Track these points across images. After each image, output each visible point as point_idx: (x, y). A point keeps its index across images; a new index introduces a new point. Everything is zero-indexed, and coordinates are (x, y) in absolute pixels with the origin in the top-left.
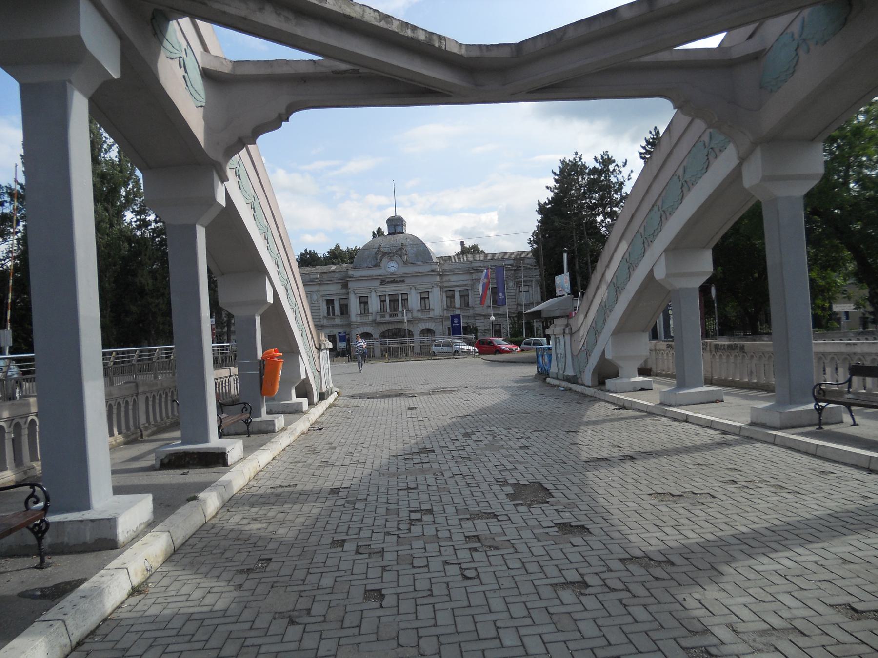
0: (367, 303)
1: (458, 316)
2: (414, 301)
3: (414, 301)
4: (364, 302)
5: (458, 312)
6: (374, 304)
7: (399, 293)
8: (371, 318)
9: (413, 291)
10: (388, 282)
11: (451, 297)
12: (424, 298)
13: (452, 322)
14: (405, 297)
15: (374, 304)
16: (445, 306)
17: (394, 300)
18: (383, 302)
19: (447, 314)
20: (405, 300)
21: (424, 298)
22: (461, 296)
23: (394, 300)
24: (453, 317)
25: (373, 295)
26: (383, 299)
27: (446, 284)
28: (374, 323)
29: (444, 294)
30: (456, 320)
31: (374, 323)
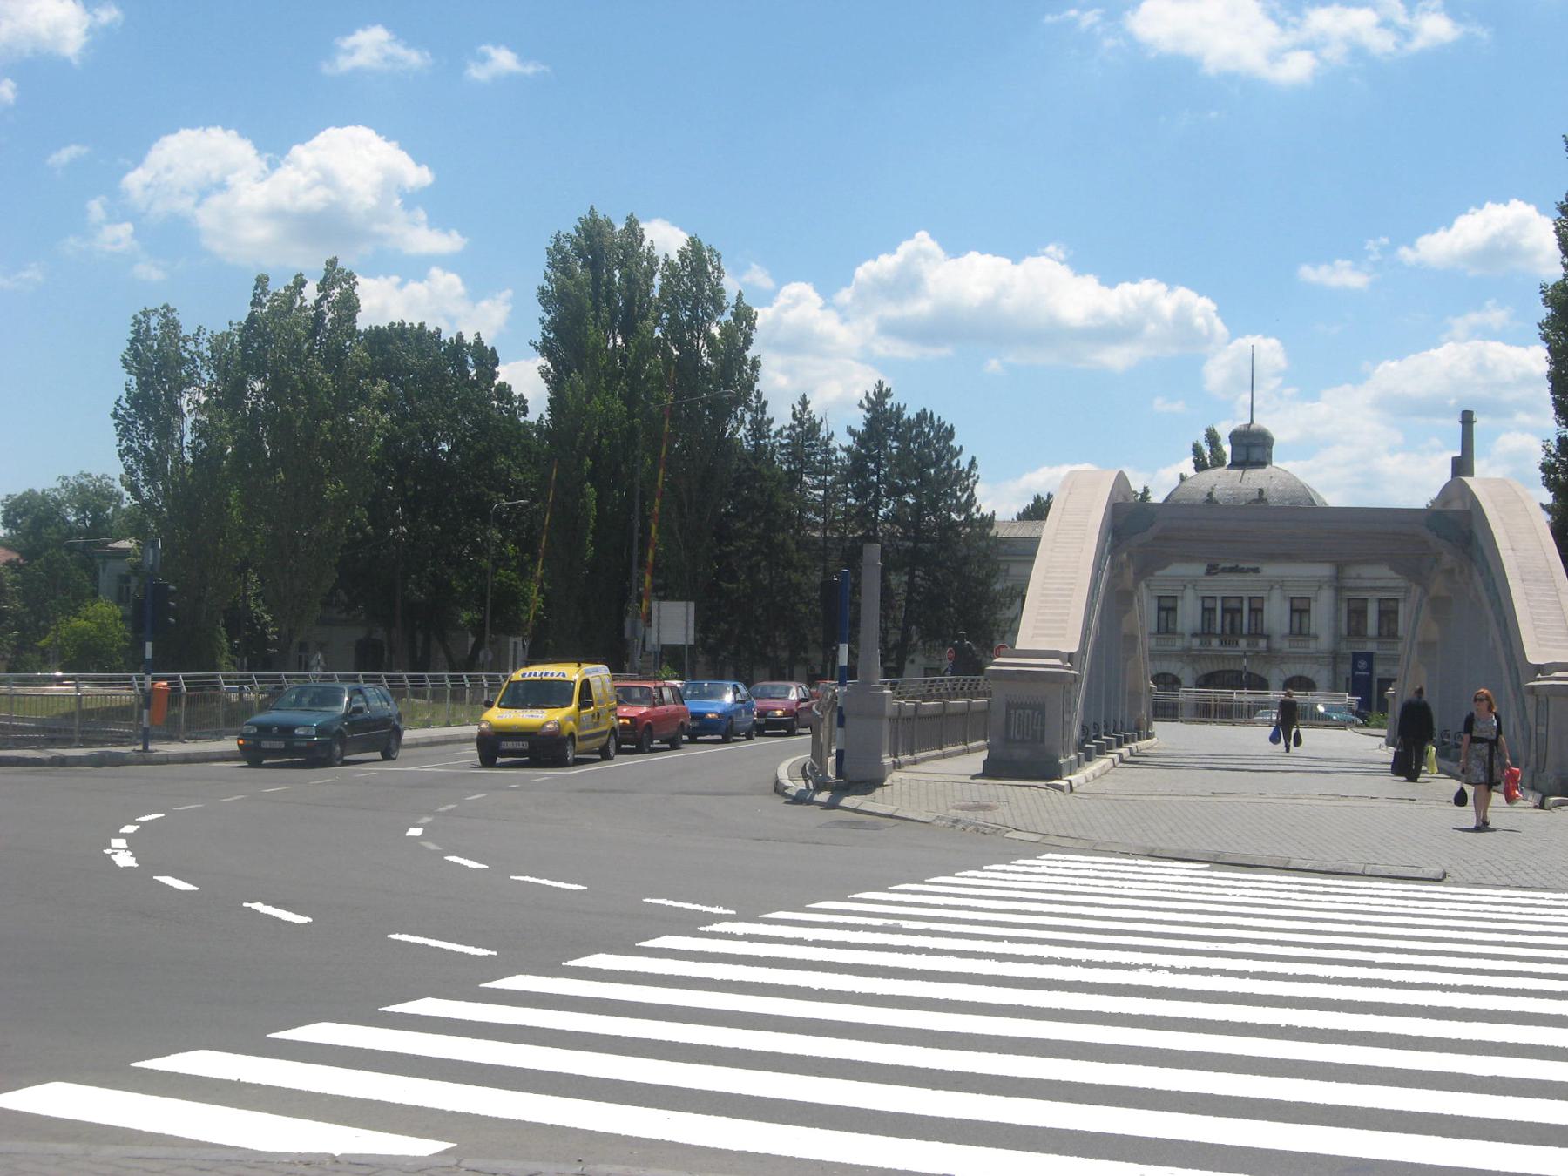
0: (1174, 609)
1: (1369, 657)
2: (1276, 615)
3: (1276, 615)
4: (1167, 608)
5: (1371, 647)
6: (1189, 615)
7: (1245, 594)
8: (1179, 644)
9: (1276, 594)
10: (1224, 570)
11: (1357, 612)
12: (1299, 610)
13: (1355, 668)
14: (1256, 605)
15: (1189, 615)
16: (1344, 631)
17: (1232, 612)
18: (1208, 612)
19: (1346, 649)
20: (1256, 611)
21: (1299, 610)
22: (1381, 614)
23: (1232, 612)
24: (1356, 657)
25: (1189, 593)
26: (1208, 604)
27: (1351, 583)
28: (1187, 655)
29: (1344, 606)
30: (1362, 664)
31: (1187, 655)
